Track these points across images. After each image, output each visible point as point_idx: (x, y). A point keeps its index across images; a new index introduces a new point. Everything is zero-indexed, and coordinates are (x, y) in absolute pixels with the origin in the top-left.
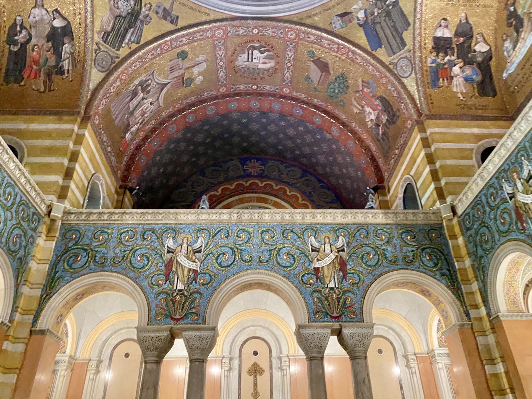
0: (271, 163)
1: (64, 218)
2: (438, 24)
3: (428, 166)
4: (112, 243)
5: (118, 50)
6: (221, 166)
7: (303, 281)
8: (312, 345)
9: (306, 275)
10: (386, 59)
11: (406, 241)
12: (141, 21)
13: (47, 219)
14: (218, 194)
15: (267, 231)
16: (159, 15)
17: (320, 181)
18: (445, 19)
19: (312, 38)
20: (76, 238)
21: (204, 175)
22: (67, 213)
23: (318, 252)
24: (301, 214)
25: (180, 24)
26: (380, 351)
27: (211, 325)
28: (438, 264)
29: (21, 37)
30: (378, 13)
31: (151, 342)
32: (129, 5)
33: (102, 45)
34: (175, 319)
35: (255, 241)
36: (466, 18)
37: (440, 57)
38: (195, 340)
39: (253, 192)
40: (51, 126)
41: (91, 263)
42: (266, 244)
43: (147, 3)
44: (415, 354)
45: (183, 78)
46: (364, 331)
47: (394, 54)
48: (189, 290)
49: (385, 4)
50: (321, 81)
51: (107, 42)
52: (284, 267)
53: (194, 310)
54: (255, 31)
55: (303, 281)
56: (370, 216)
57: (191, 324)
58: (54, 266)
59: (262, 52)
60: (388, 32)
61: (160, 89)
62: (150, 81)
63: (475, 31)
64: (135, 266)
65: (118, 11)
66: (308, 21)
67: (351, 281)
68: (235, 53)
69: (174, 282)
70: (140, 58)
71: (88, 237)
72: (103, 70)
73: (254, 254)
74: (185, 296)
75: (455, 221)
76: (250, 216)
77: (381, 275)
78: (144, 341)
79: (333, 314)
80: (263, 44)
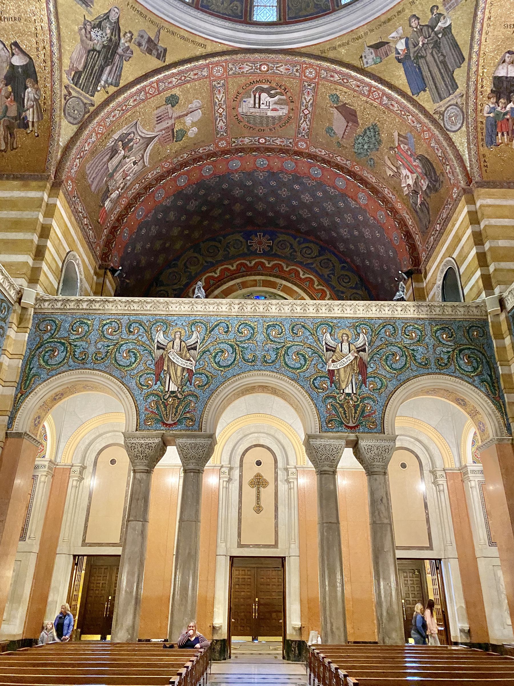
1: (37, 306)
2: (501, 59)
3: (474, 249)
4: (94, 336)
5: (93, 96)
6: (220, 242)
7: (315, 386)
8: (323, 457)
9: (319, 378)
11: (441, 340)
12: (121, 56)
13: (17, 307)
14: (216, 276)
15: (274, 326)
16: (142, 47)
17: (342, 262)
19: (337, 77)
20: (51, 329)
22: (39, 300)
23: (334, 351)
24: (315, 306)
25: (169, 59)
26: (404, 466)
27: (208, 432)
28: (477, 369)
30: (423, 44)
31: (140, 449)
32: (104, 35)
33: (74, 89)
34: (167, 425)
35: (260, 337)
37: (500, 104)
38: (189, 448)
39: (259, 274)
40: (17, 194)
41: (70, 360)
42: (272, 341)
43: (127, 31)
44: (444, 470)
45: (173, 130)
48: (183, 392)
49: (433, 30)
50: (346, 133)
51: (78, 86)
52: (293, 368)
53: (188, 415)
54: (264, 68)
55: (315, 386)
56: (399, 309)
57: (186, 430)
58: (28, 361)
59: (272, 96)
60: (435, 71)
61: (143, 146)
62: (132, 135)
64: (121, 363)
66: (331, 55)
67: (372, 386)
68: (238, 98)
69: (165, 382)
70: (119, 105)
71: (65, 328)
72: (75, 122)
73: (257, 353)
74: (178, 399)
75: (503, 317)
76: (253, 308)
77: (408, 380)
78: (133, 448)
79: (348, 423)
80: (274, 85)
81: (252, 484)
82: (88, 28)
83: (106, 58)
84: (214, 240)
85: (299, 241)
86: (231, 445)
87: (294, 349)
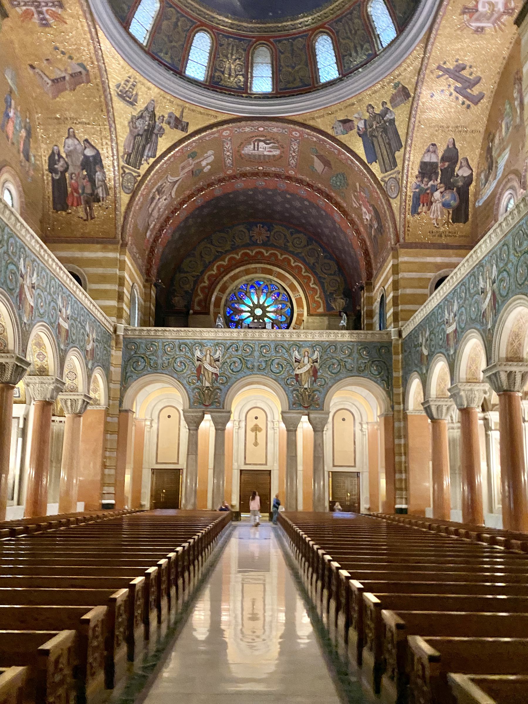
18: (434, 145)
29: (59, 166)
33: (127, 168)
35: (256, 354)
36: (454, 144)
47: (386, 171)
65: (136, 130)
70: (157, 171)
73: (255, 364)
81: (252, 430)
82: (134, 120)
83: (147, 139)
86: (240, 407)
87: (276, 361)
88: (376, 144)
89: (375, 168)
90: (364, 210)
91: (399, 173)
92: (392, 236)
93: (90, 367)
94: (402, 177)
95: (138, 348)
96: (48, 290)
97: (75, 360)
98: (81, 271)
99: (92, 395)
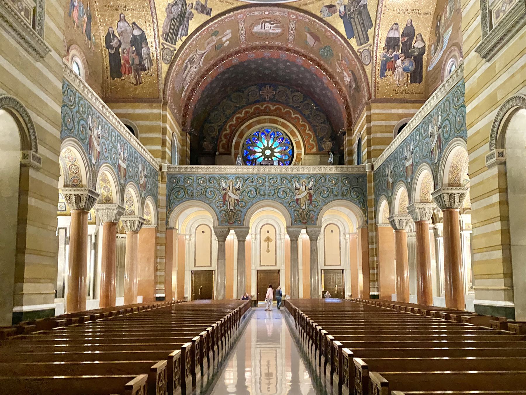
0: (280, 88)
10: (356, 48)
14: (242, 116)
18: (396, 24)
21: (231, 100)
46: (317, 229)
54: (267, 13)
60: (359, 28)
63: (416, 33)
68: (253, 25)
77: (329, 202)
84: (239, 91)
85: (291, 91)
88: (353, 23)
89: (353, 42)
90: (345, 74)
91: (371, 46)
92: (366, 94)
93: (143, 196)
94: (373, 48)
95: (178, 181)
96: (110, 140)
97: (131, 191)
98: (134, 124)
99: (145, 217)
